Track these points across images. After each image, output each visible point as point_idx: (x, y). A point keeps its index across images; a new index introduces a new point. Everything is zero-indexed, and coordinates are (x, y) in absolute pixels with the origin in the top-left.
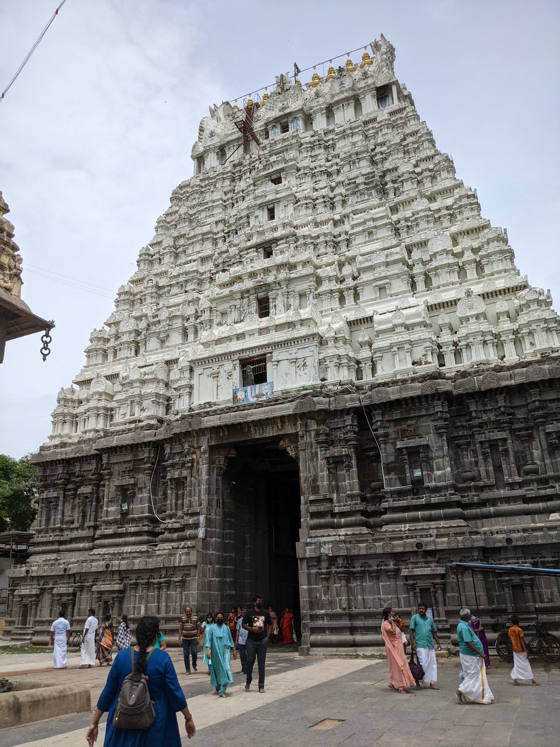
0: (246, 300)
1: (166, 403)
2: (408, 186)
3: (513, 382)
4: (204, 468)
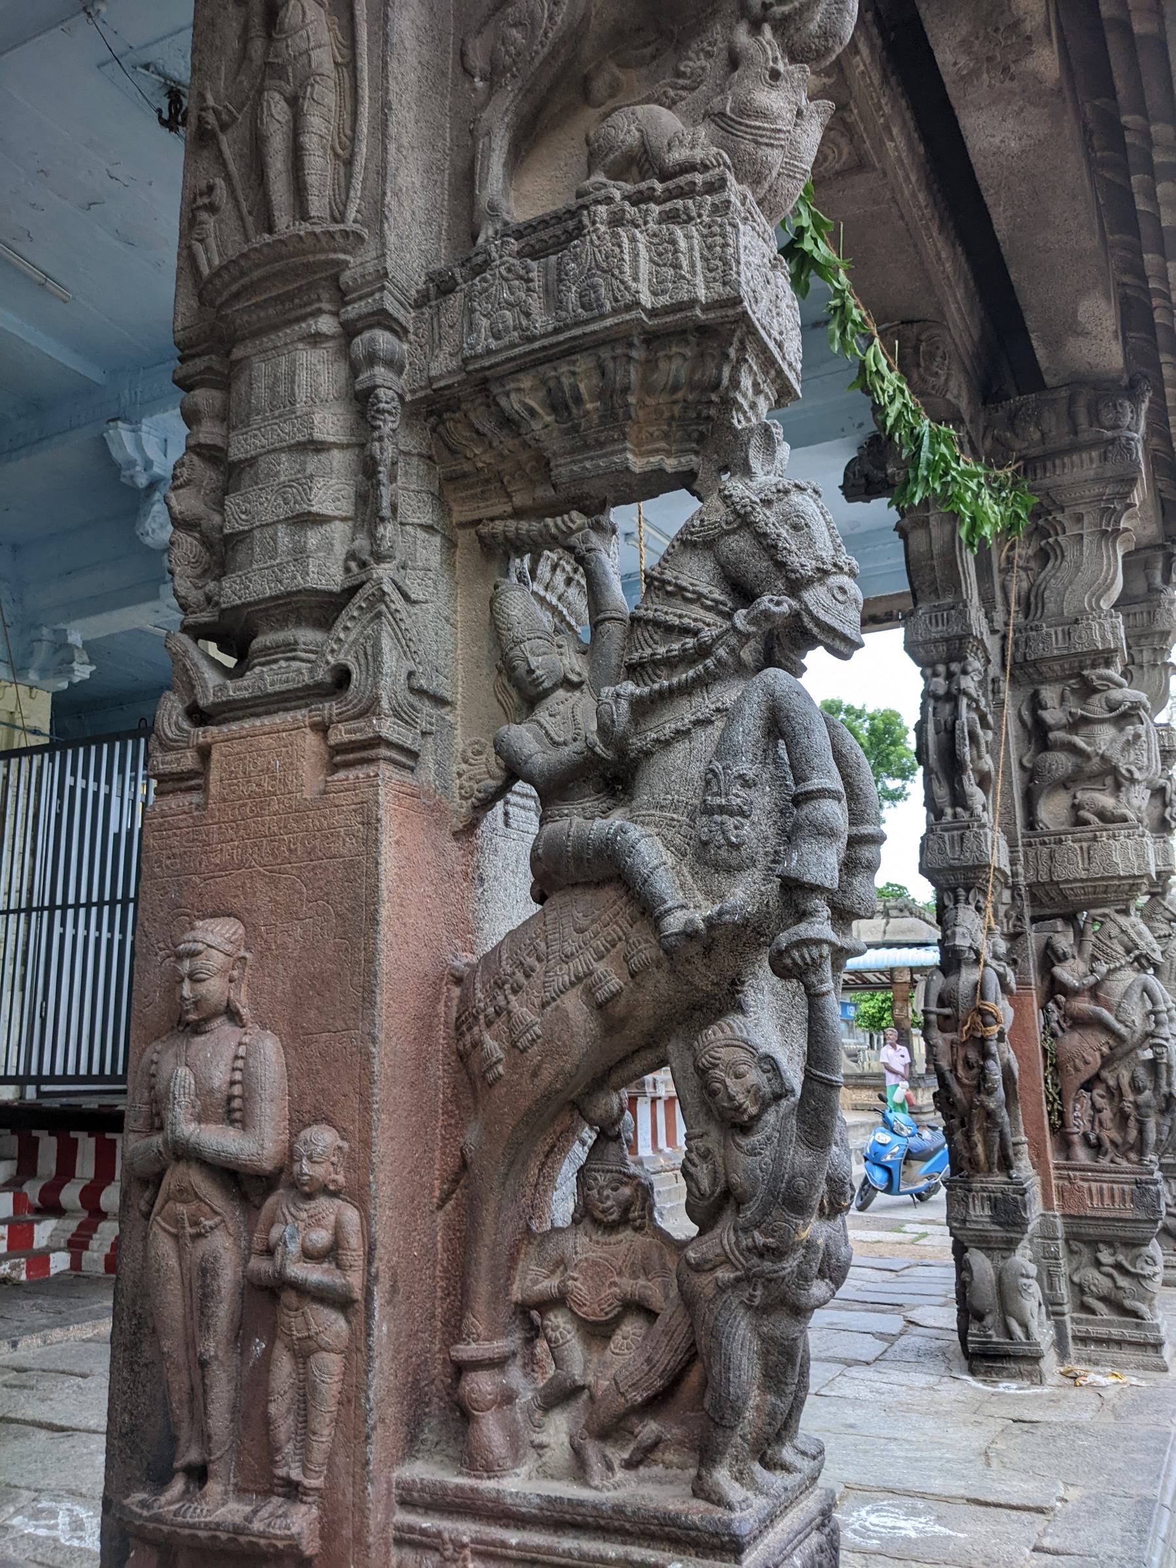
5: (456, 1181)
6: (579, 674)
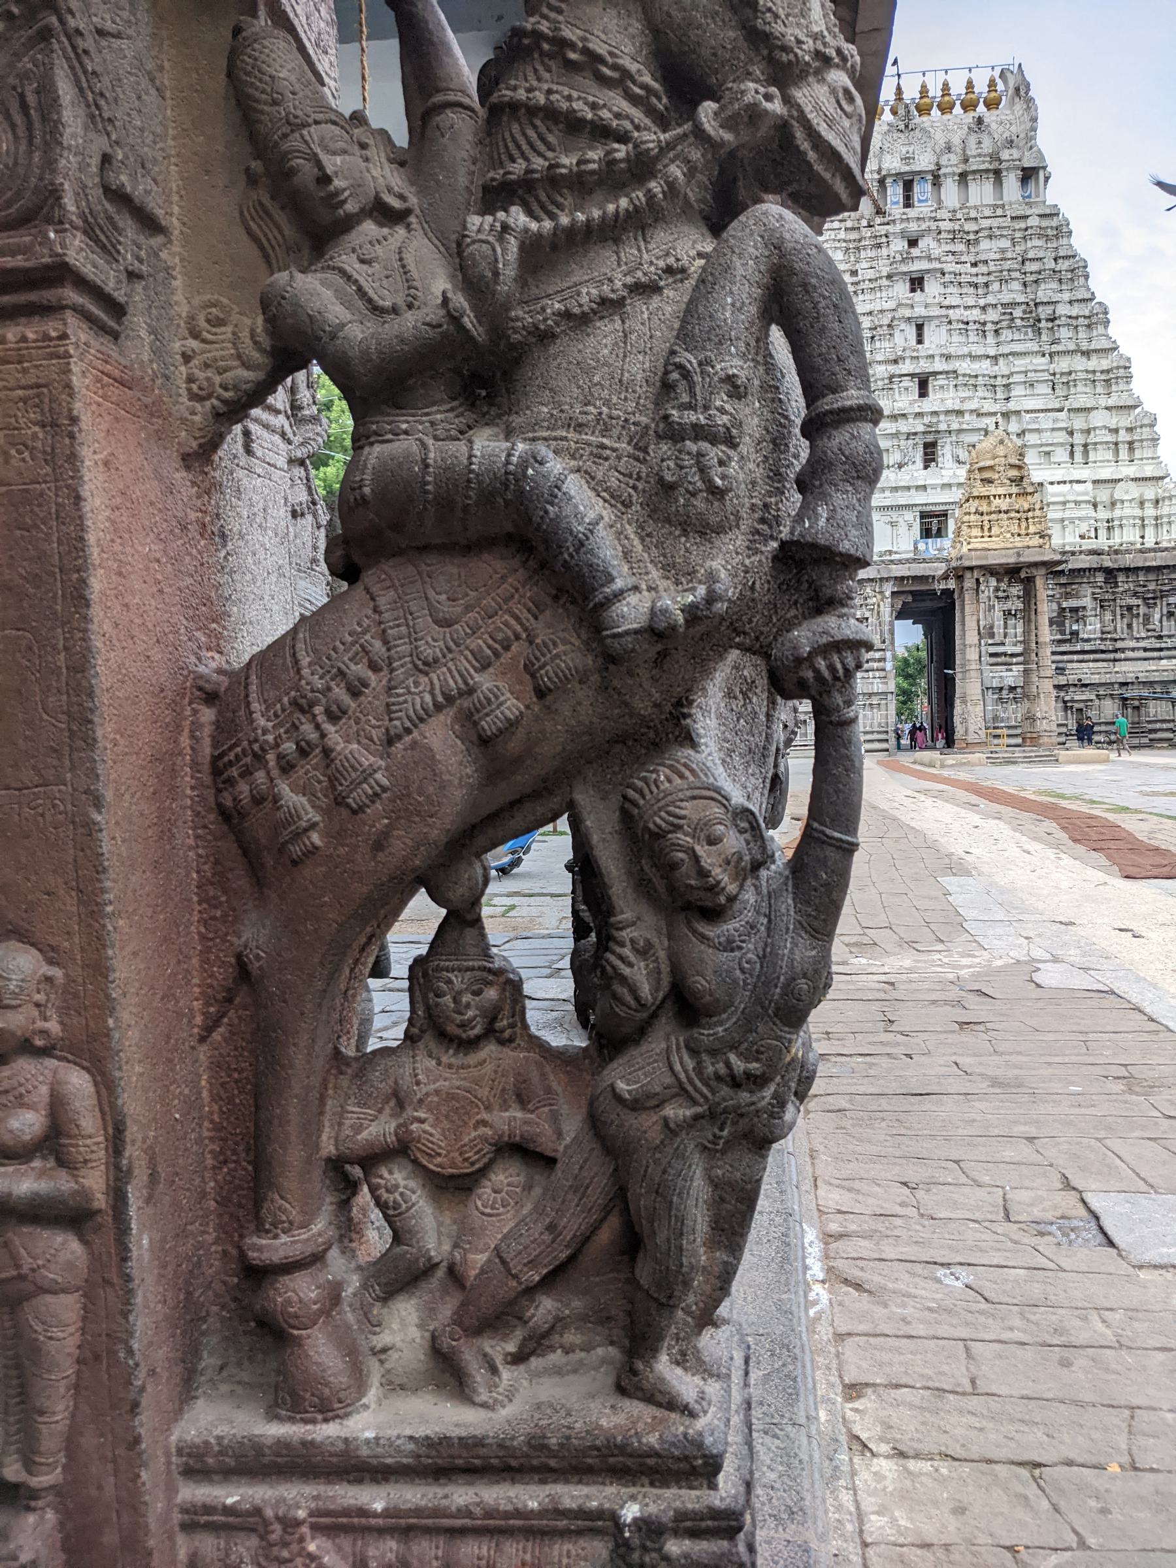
0: (910, 442)
2: (1064, 333)
3: (1154, 564)
4: (886, 610)
5: (229, 1000)
6: (402, 197)
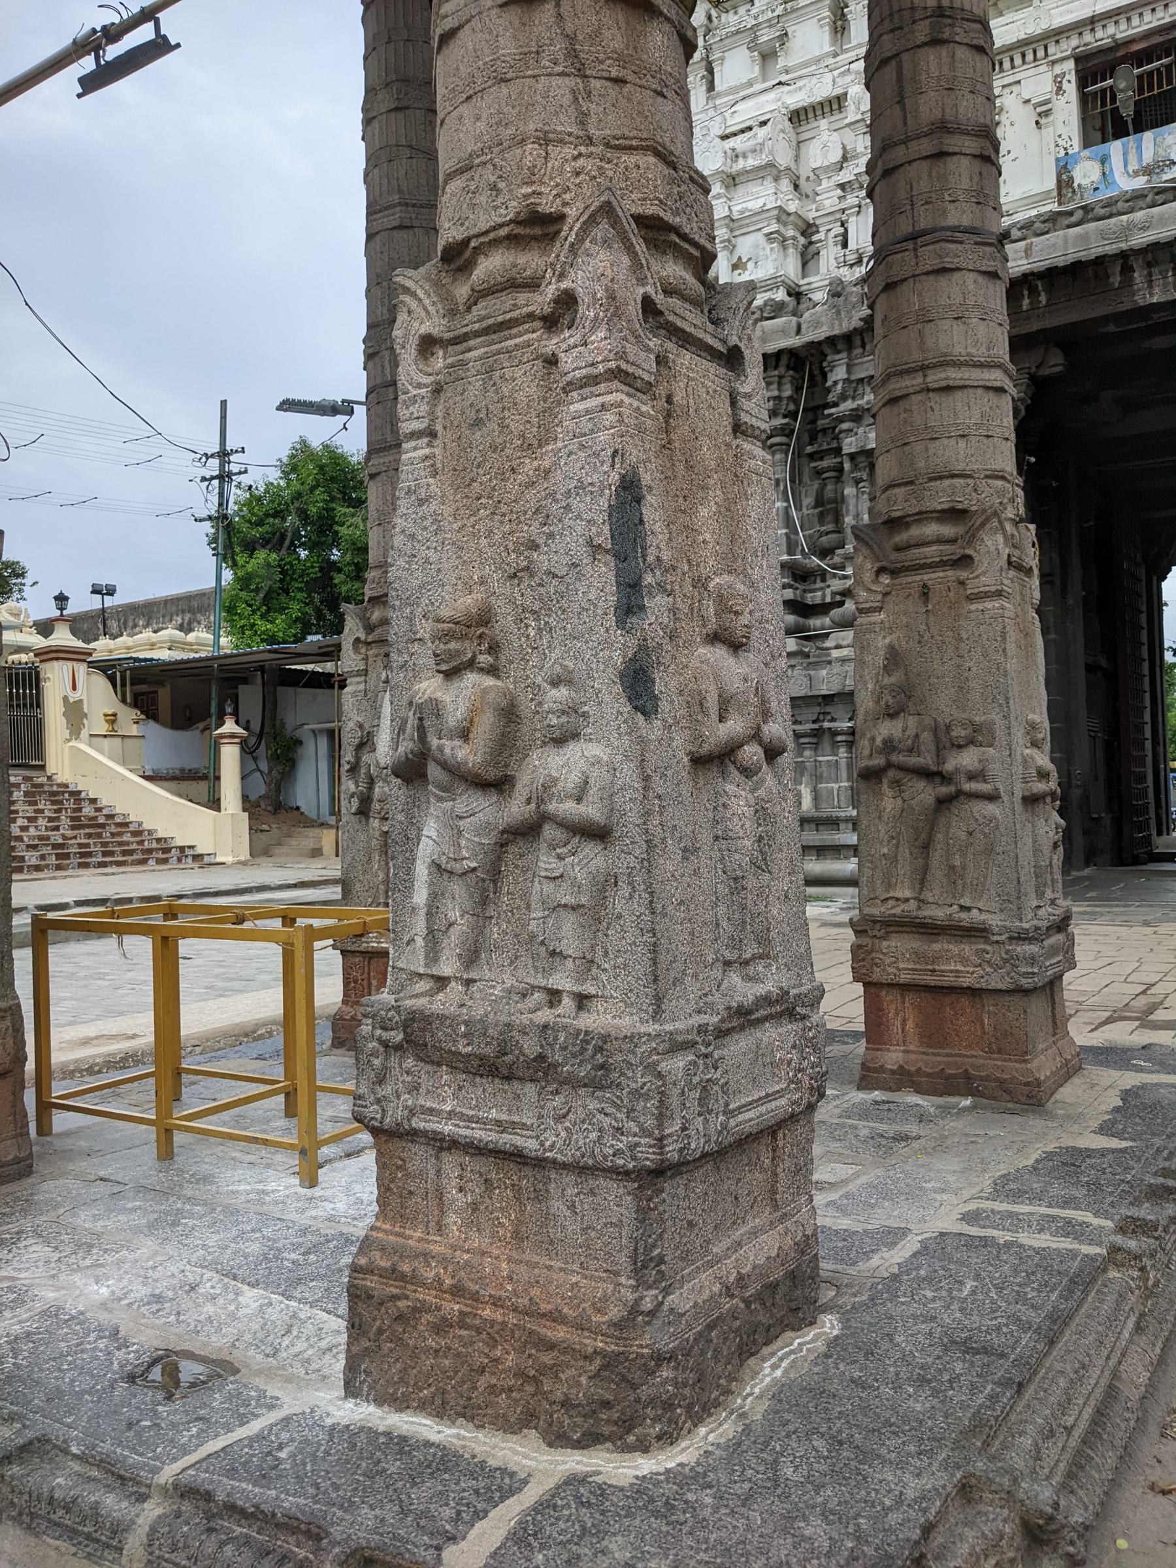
1: (802, 240)
